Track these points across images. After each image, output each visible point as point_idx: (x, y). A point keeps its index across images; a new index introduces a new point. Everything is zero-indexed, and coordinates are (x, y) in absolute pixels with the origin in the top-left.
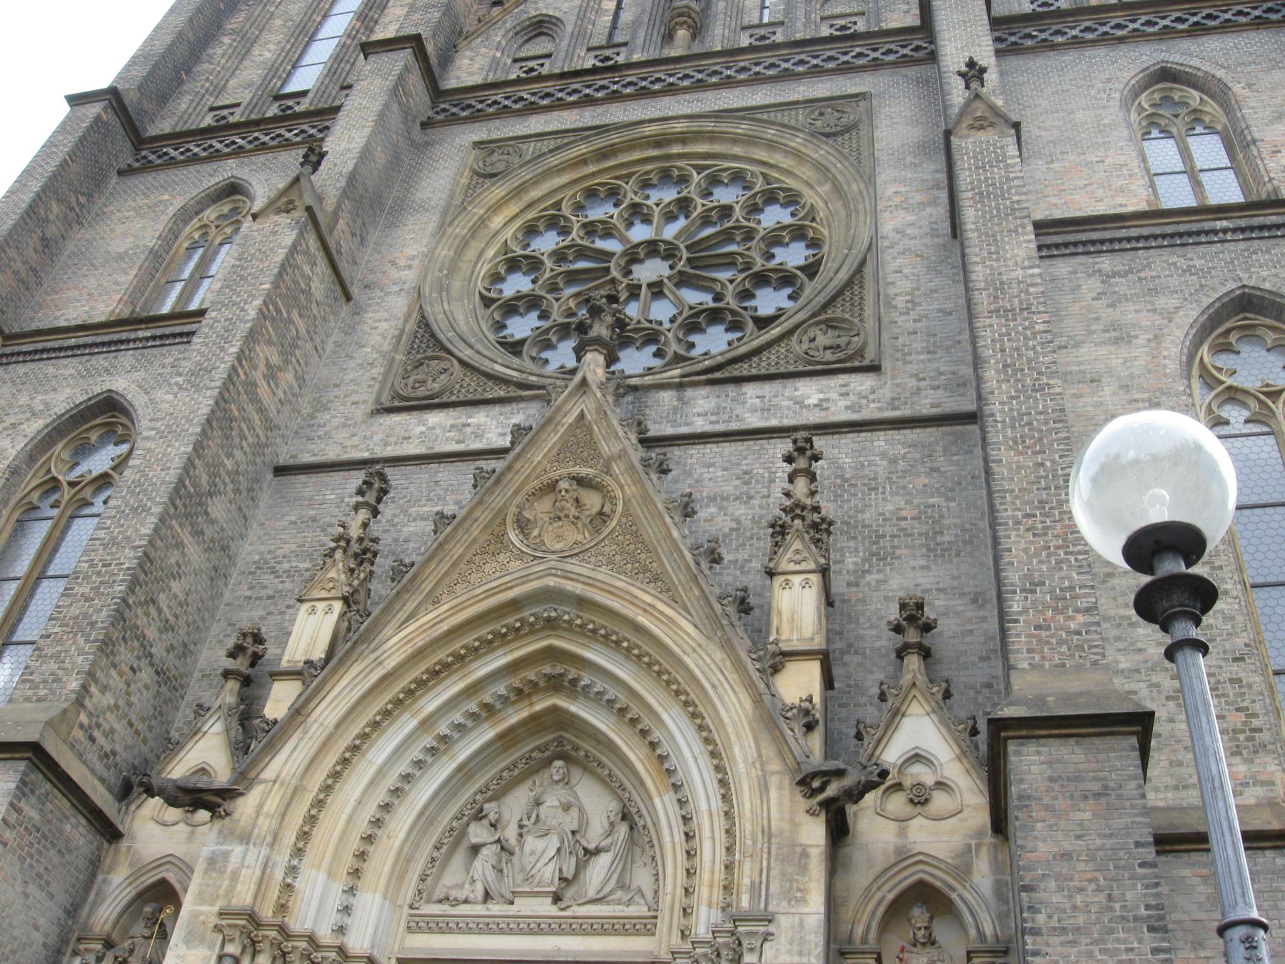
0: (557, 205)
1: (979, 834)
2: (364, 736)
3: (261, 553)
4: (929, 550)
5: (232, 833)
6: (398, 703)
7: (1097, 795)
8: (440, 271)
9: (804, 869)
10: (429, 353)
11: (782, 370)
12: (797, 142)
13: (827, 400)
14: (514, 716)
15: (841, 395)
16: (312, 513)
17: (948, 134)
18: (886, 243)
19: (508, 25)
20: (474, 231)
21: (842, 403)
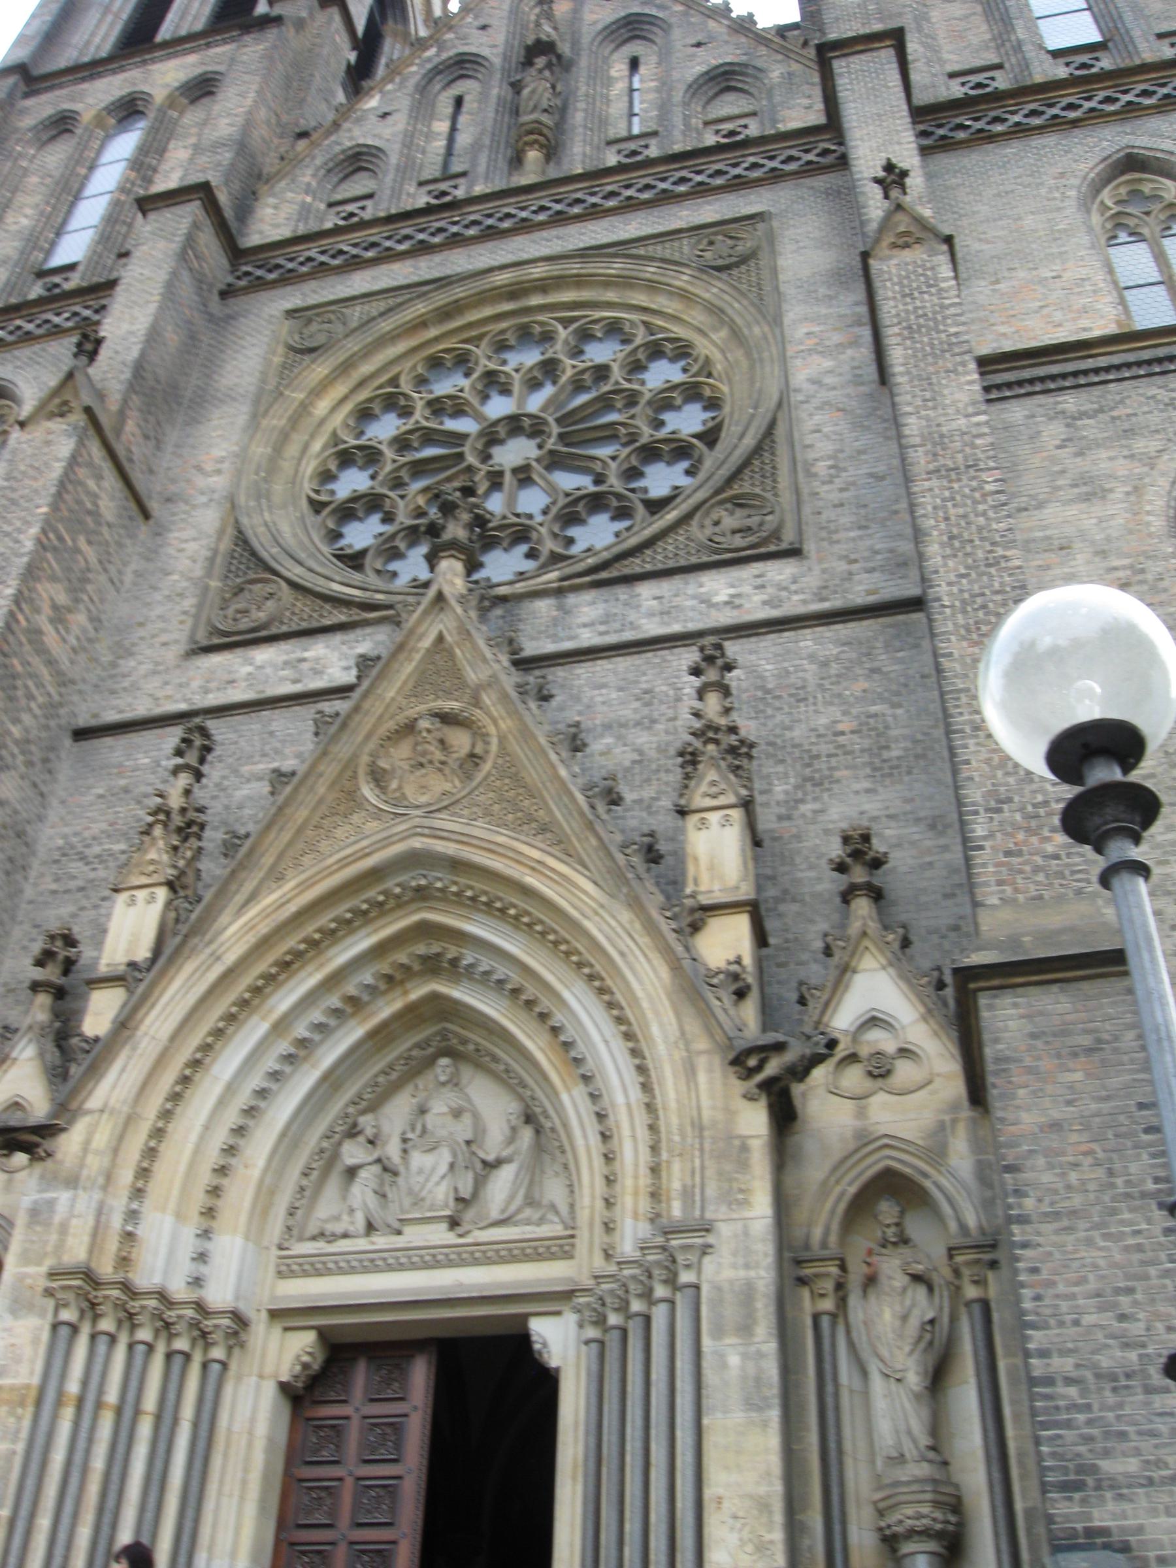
0: (394, 381)
1: (954, 1107)
2: (206, 1048)
3: (65, 837)
4: (875, 769)
5: (55, 1178)
6: (243, 1004)
7: (1090, 1051)
8: (257, 474)
9: (743, 1165)
10: (252, 575)
11: (682, 563)
12: (683, 280)
13: (739, 595)
14: (386, 1009)
15: (756, 588)
16: (123, 782)
17: (865, 256)
18: (800, 397)
19: (318, 161)
20: (295, 421)
21: (758, 598)
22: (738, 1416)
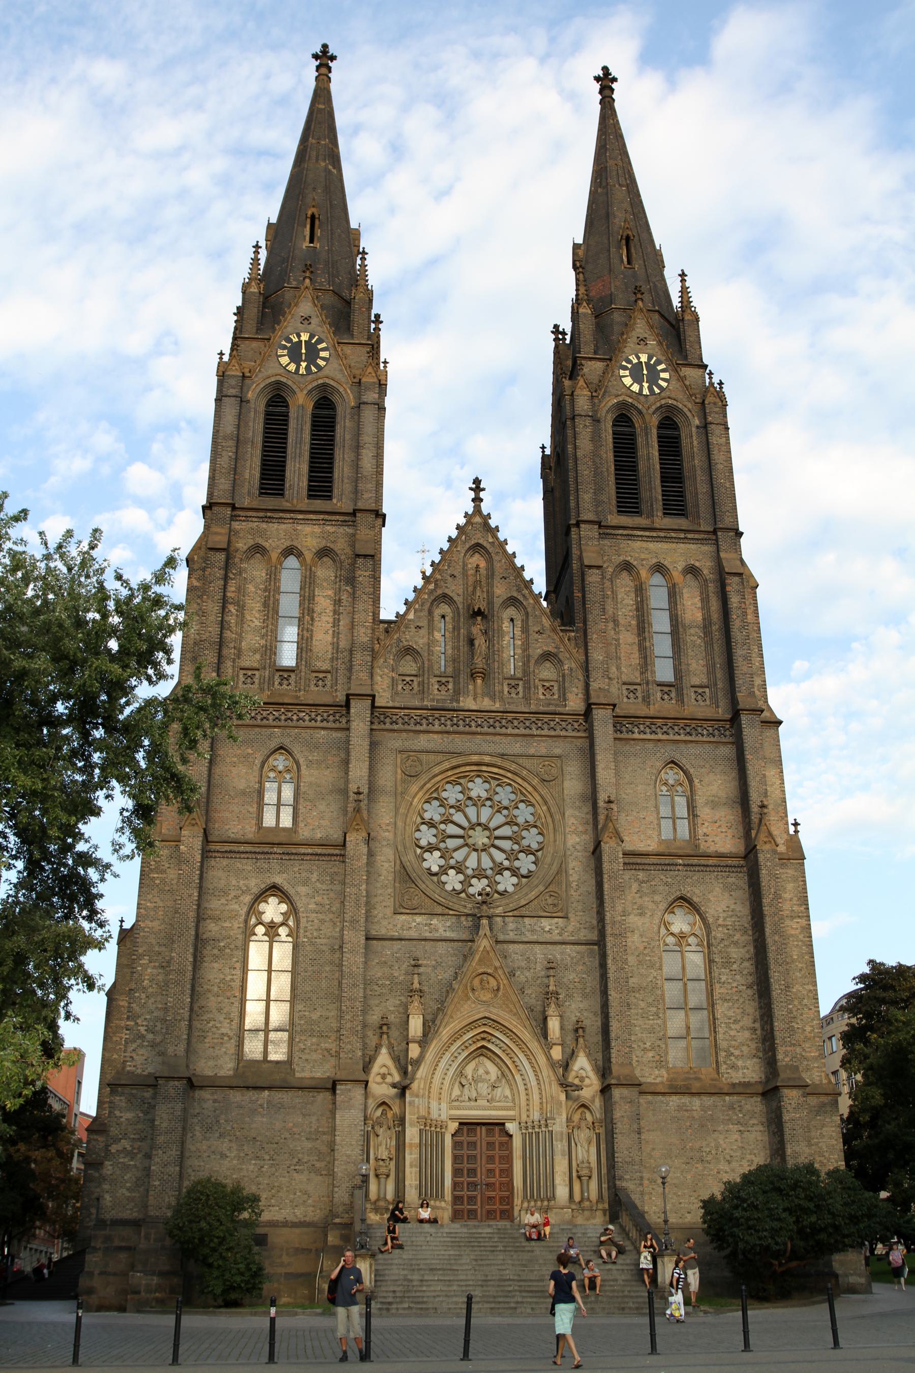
9: (561, 1107)
22: (560, 1157)
